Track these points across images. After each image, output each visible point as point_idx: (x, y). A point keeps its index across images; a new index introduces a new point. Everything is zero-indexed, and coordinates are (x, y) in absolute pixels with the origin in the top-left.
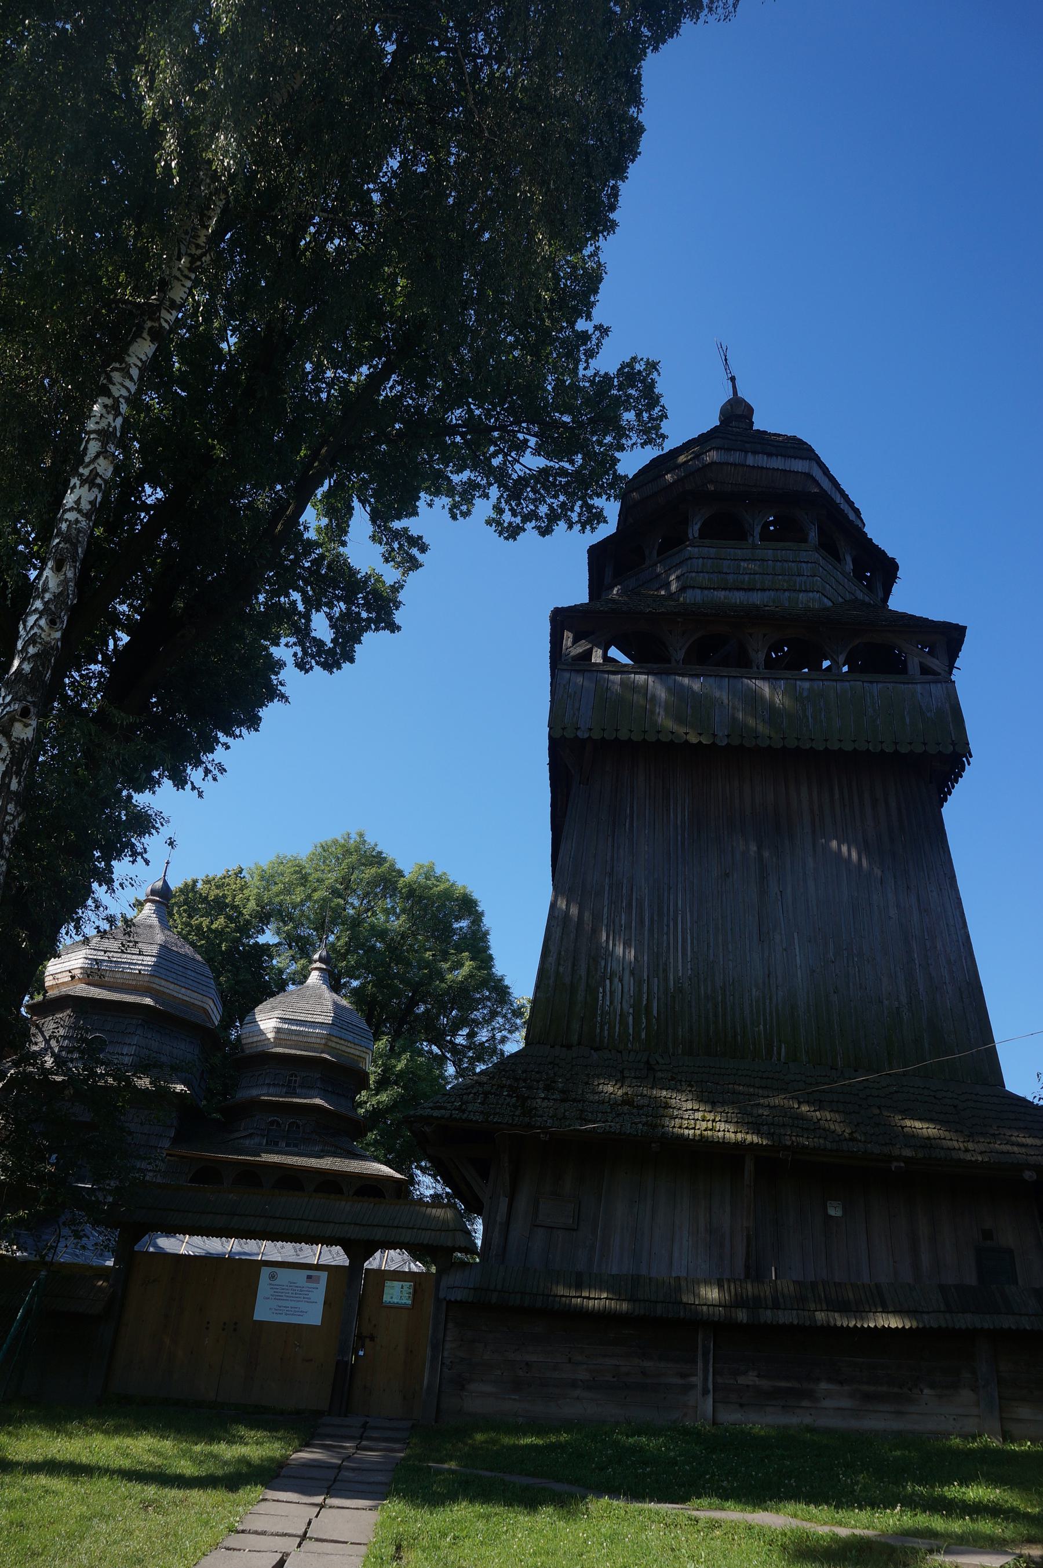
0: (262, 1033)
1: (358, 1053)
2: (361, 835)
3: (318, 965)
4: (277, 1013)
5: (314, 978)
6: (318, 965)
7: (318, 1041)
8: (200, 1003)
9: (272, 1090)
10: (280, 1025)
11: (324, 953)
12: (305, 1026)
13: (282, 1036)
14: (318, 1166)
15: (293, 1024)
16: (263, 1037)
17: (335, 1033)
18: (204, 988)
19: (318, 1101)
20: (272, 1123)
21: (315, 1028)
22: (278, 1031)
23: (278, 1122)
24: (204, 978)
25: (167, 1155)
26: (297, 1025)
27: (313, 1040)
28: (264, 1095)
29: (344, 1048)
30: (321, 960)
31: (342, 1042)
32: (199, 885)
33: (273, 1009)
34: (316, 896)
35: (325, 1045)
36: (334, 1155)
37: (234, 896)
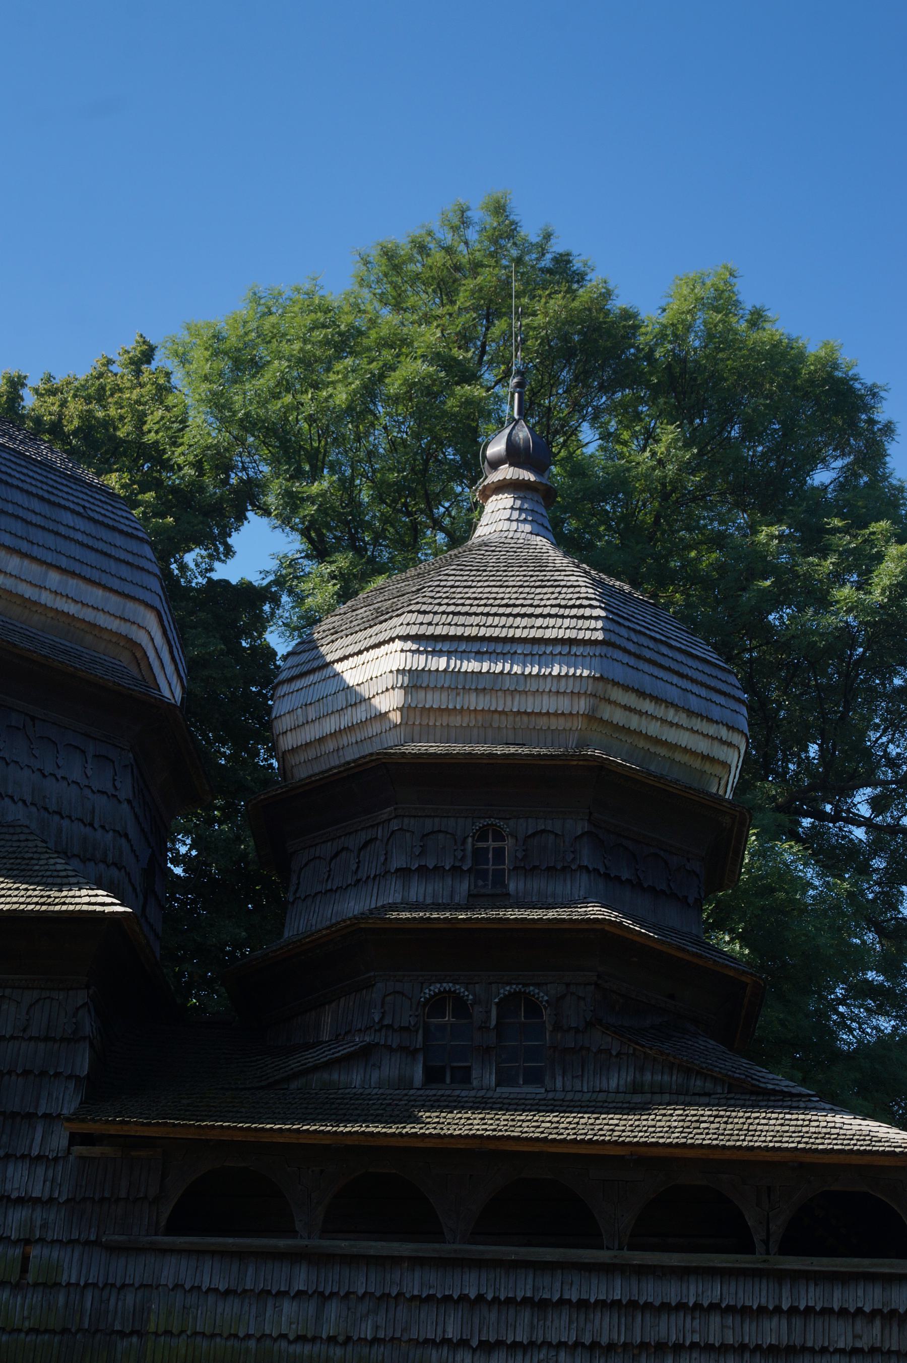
0: (354, 699)
1: (703, 746)
2: (499, 209)
3: (506, 472)
4: (397, 625)
5: (498, 517)
6: (506, 472)
7: (564, 704)
8: (114, 625)
9: (417, 891)
10: (420, 662)
11: (523, 433)
12: (511, 656)
13: (433, 700)
14: (641, 1137)
15: (463, 655)
16: (360, 714)
17: (618, 673)
18: (125, 571)
19: (595, 911)
20: (437, 1005)
21: (542, 659)
22: (414, 681)
23: (459, 1001)
24: (119, 540)
25: (75, 1139)
26: (479, 655)
27: (548, 704)
28: (394, 907)
29: (653, 728)
30: (514, 455)
31: (647, 706)
32: (29, 400)
33: (381, 616)
34: (394, 385)
35: (591, 717)
36: (685, 1097)
37: (141, 419)
